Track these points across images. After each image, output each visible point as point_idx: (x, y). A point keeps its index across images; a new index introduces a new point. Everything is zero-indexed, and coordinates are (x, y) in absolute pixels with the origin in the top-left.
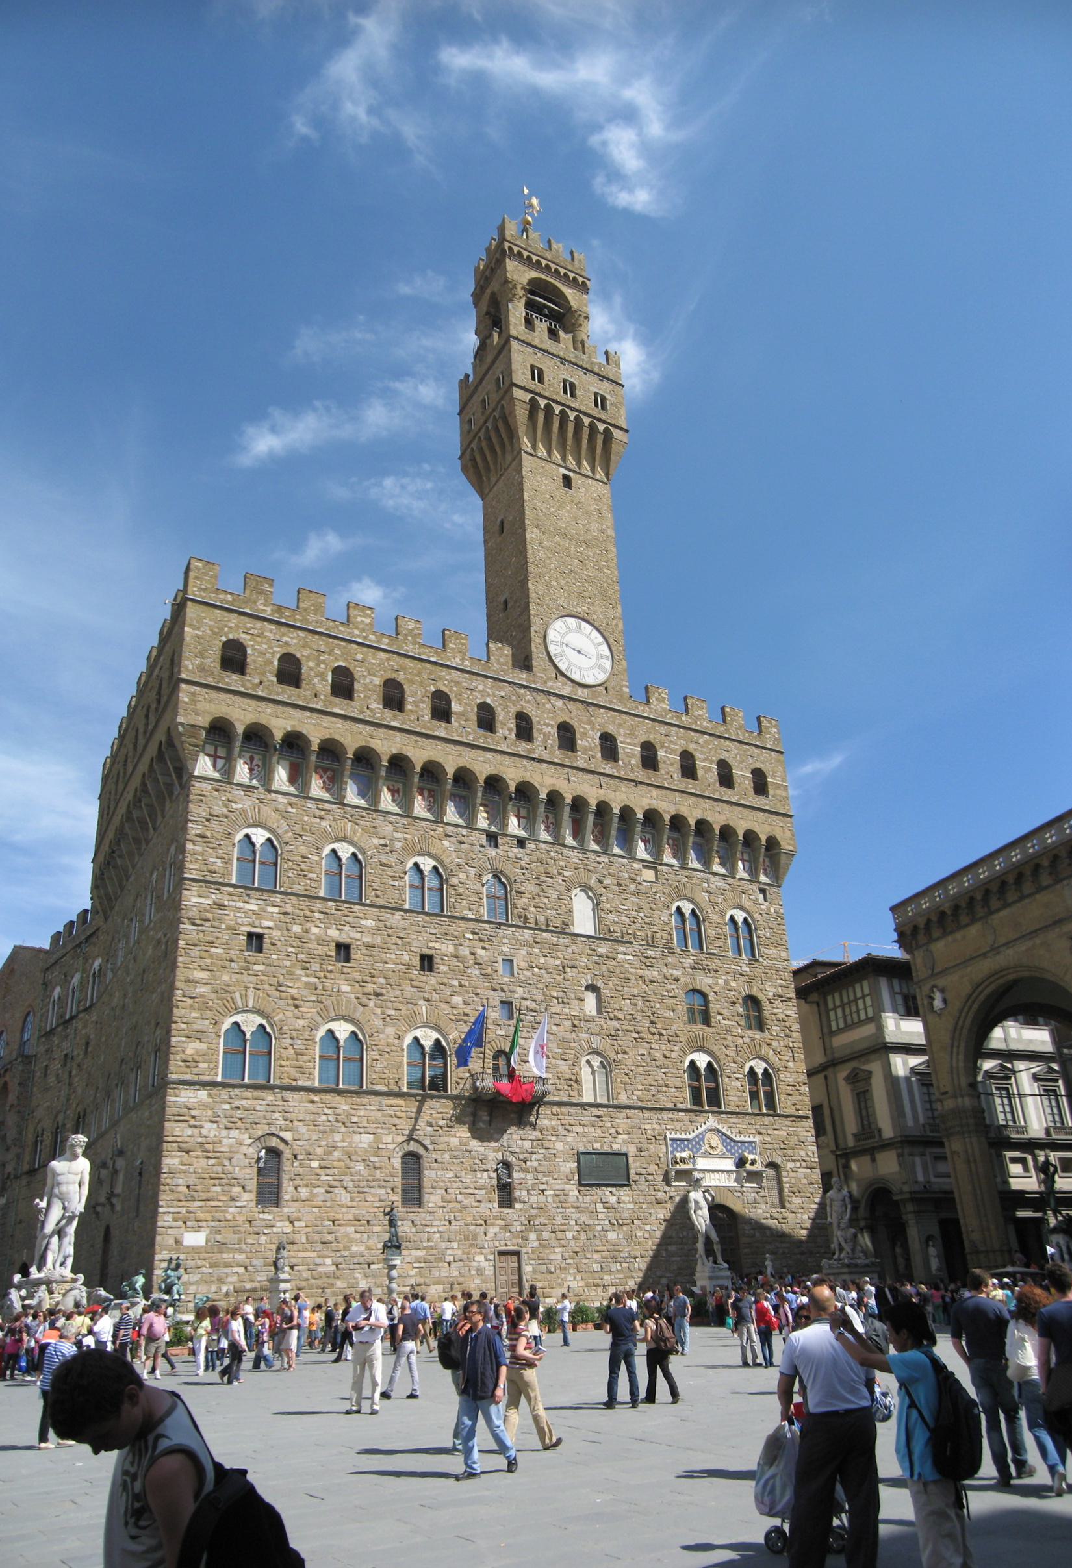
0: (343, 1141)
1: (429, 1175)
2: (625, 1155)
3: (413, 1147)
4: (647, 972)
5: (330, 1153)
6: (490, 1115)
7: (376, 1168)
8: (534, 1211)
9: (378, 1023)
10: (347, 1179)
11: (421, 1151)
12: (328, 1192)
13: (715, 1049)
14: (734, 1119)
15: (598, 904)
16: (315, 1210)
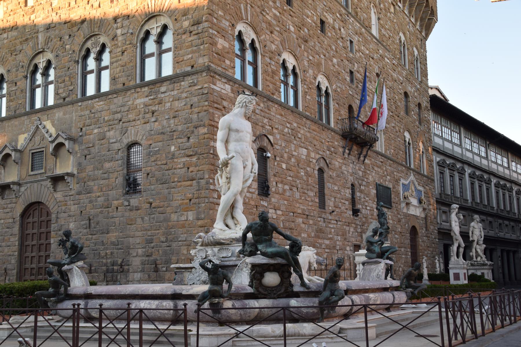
0: (295, 151)
1: (328, 185)
2: (390, 189)
3: (322, 164)
4: (393, 74)
5: (290, 159)
6: (350, 150)
7: (310, 176)
8: (364, 219)
9: (306, 63)
10: (298, 182)
11: (326, 168)
12: (291, 190)
13: (412, 131)
14: (417, 177)
15: (379, 19)
16: (286, 202)
